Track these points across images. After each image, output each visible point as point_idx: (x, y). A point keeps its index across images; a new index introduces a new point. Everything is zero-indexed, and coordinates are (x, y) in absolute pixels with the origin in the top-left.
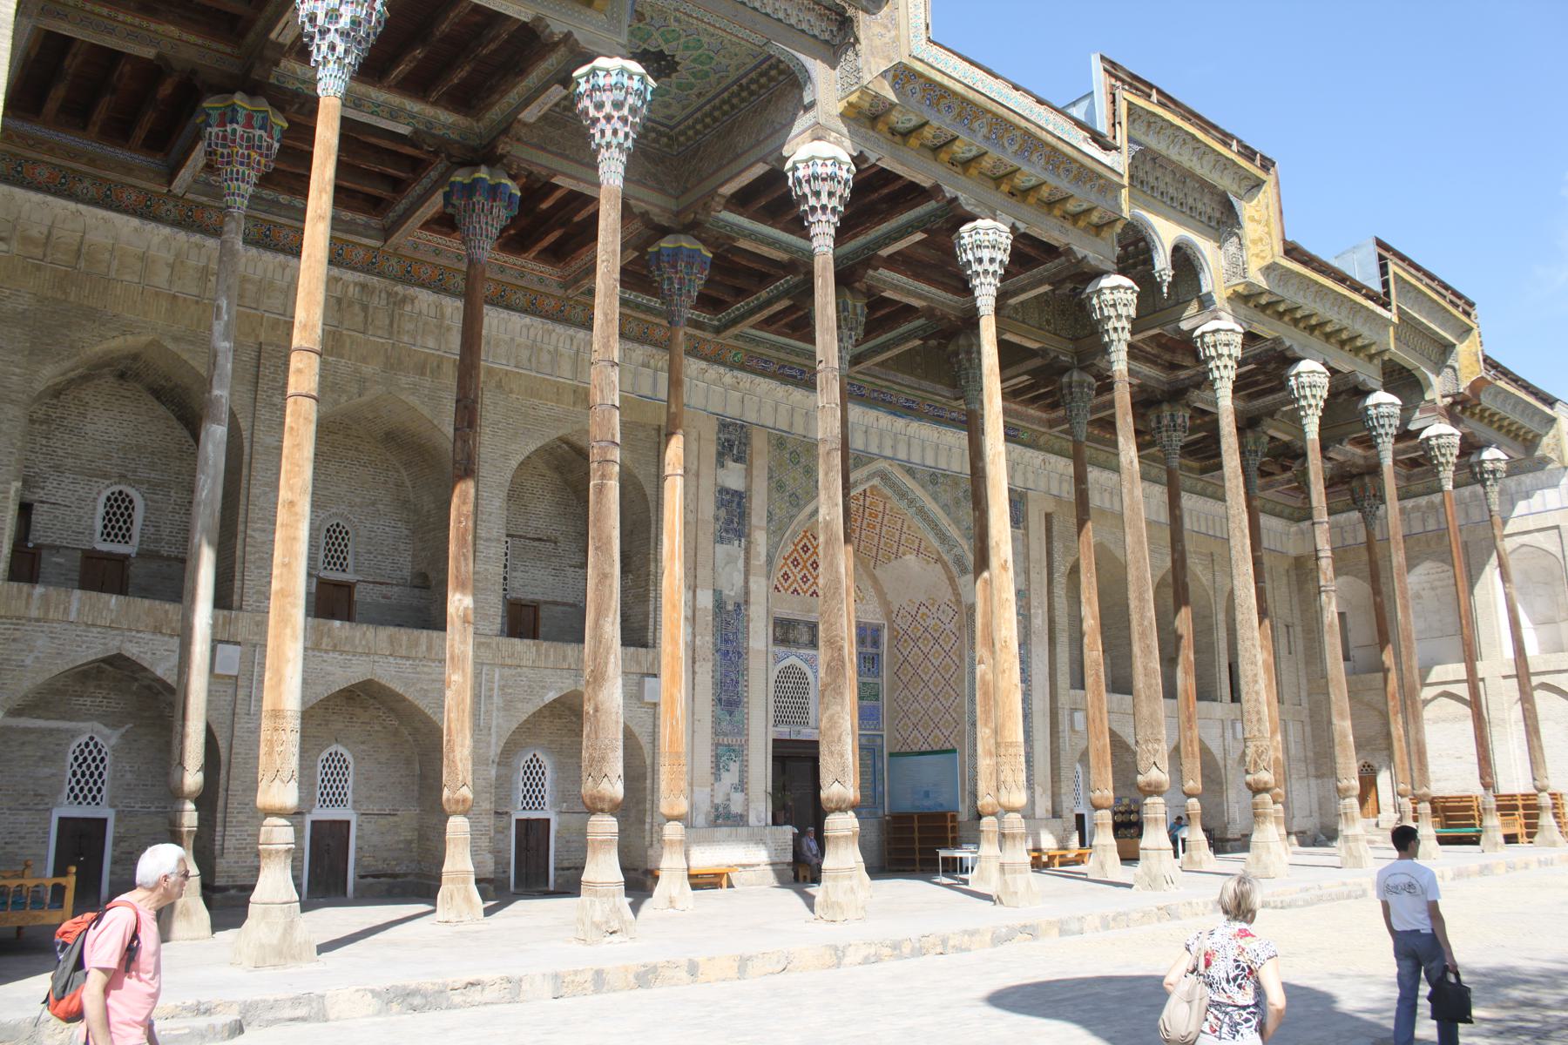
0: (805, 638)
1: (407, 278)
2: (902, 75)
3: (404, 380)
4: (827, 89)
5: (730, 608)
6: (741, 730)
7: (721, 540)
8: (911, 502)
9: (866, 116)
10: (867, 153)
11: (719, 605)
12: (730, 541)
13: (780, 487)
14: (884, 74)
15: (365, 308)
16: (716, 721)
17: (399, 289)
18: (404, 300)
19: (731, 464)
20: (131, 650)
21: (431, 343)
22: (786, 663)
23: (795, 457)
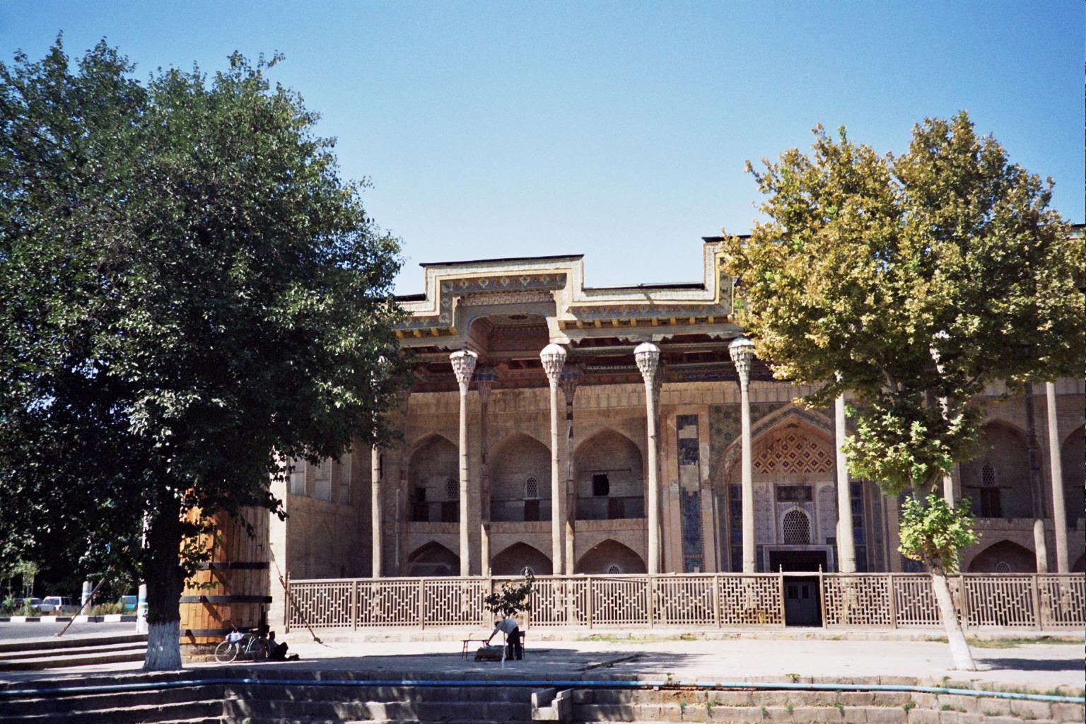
0: (803, 495)
1: (517, 386)
2: (575, 310)
3: (524, 425)
4: (553, 324)
5: (691, 494)
6: (700, 551)
7: (684, 464)
8: (818, 422)
9: (568, 327)
10: (575, 339)
11: (683, 493)
12: (689, 463)
13: (719, 431)
14: (568, 311)
15: (504, 401)
16: (685, 548)
17: (516, 390)
18: (520, 393)
19: (687, 427)
20: (437, 540)
21: (532, 408)
22: (791, 510)
23: (727, 415)
